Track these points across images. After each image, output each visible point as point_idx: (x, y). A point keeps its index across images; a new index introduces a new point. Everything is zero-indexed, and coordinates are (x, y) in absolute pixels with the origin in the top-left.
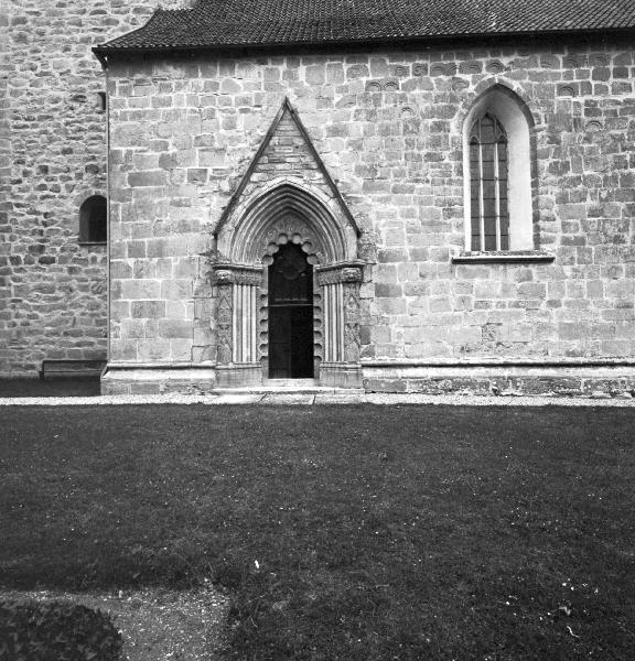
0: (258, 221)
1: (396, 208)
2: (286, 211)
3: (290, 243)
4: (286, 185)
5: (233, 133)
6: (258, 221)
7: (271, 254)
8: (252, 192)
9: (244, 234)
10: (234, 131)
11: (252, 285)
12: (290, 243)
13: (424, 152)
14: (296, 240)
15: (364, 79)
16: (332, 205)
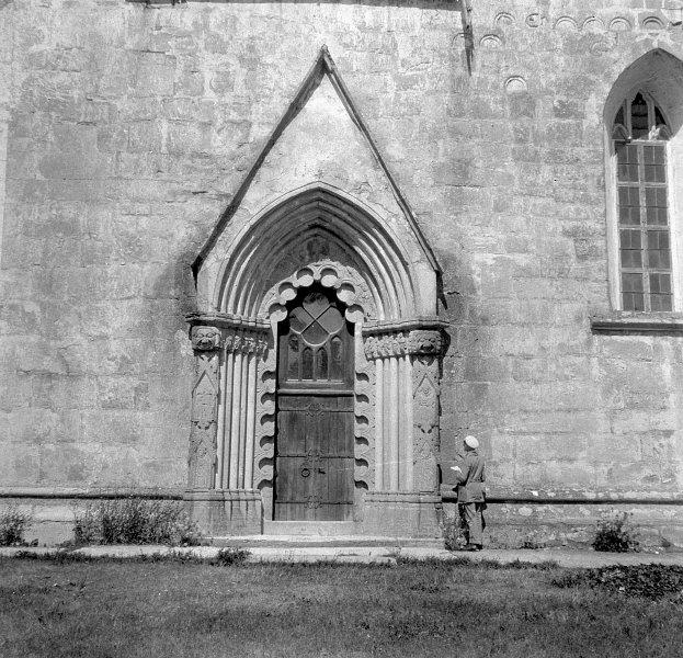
2: (316, 231)
3: (317, 284)
5: (228, 98)
7: (283, 302)
8: (257, 203)
13: (544, 151)
14: (328, 281)
16: (396, 225)
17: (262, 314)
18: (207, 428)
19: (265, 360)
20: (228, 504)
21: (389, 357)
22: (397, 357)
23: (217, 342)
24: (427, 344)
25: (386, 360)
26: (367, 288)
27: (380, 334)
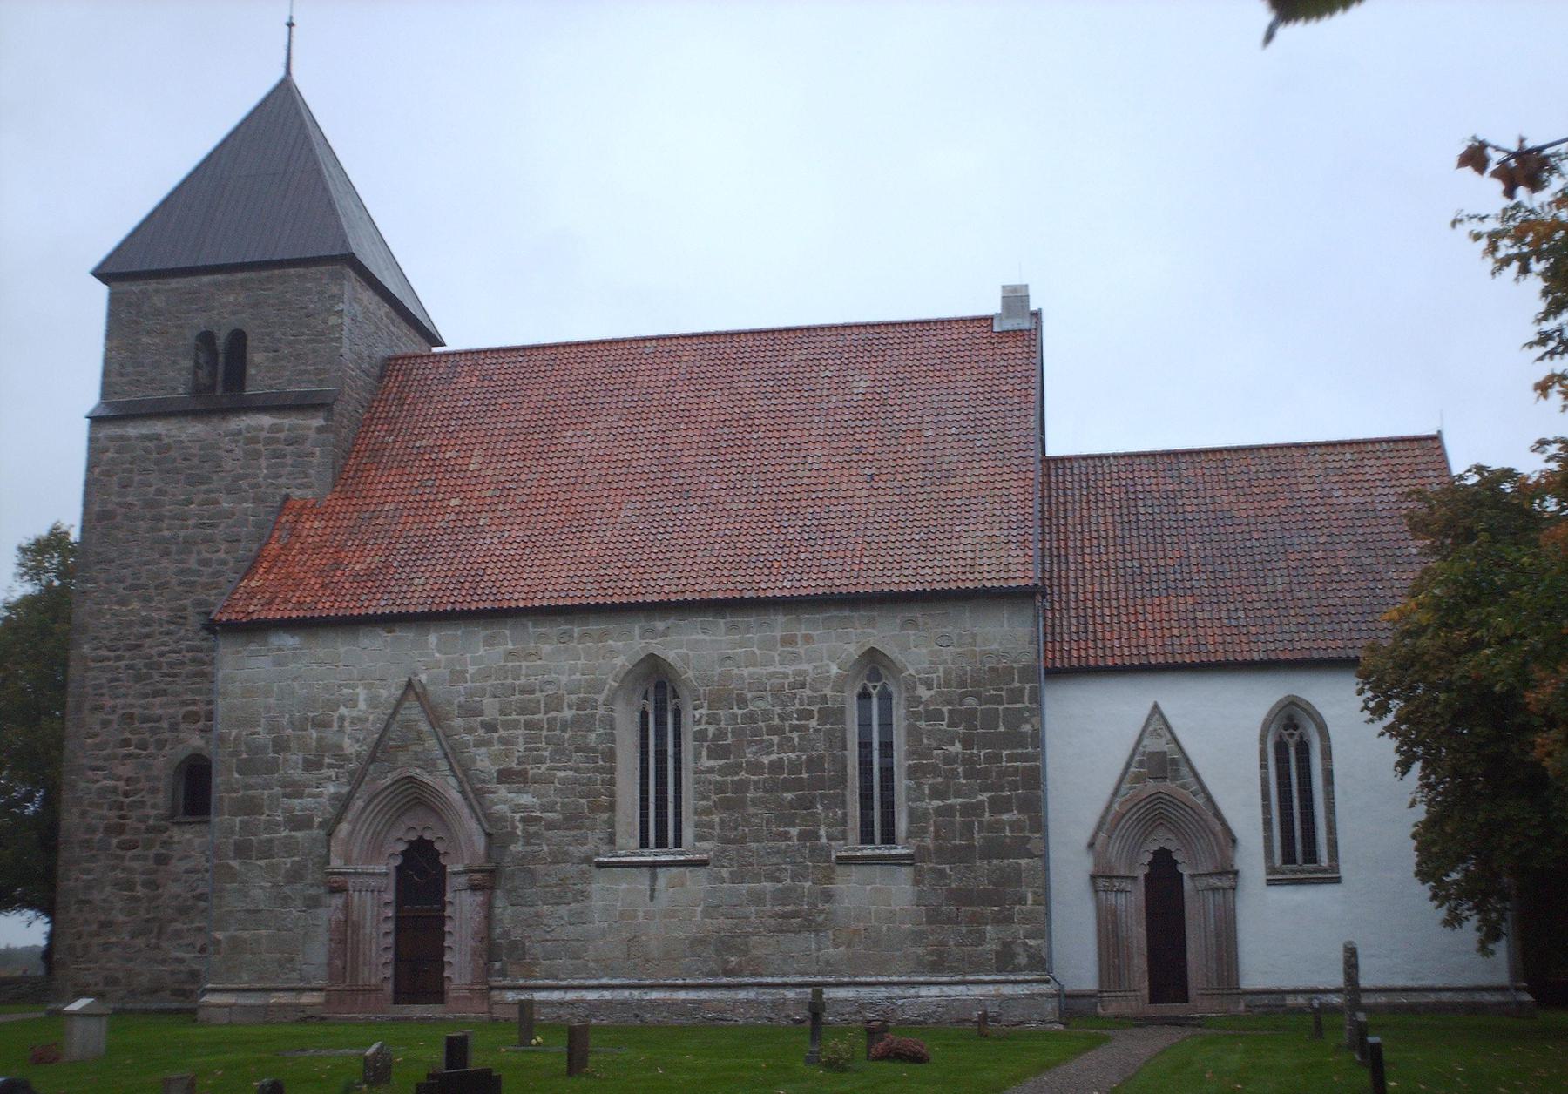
0: (380, 816)
1: (535, 800)
3: (421, 838)
4: (411, 777)
6: (380, 816)
9: (362, 832)
11: (372, 891)
12: (421, 838)
14: (428, 836)
15: (500, 649)
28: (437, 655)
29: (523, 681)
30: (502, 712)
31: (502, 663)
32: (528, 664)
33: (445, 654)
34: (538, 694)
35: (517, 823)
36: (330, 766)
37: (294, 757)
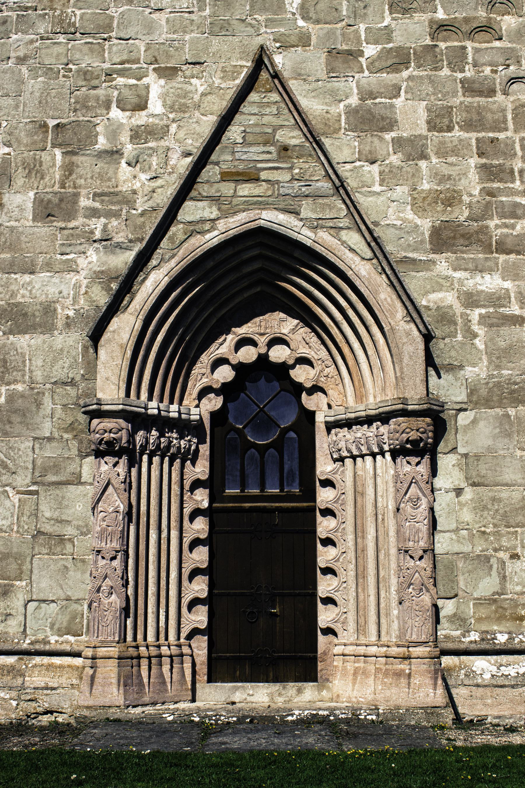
1: (508, 284)
10: (144, 113)
17: (189, 400)
18: (113, 558)
19: (193, 464)
20: (144, 663)
21: (362, 456)
22: (374, 455)
23: (124, 440)
24: (414, 435)
25: (359, 460)
26: (330, 362)
27: (349, 424)
28: (301, 23)
29: (469, 73)
30: (432, 126)
31: (428, 41)
32: (477, 45)
33: (318, 22)
34: (500, 97)
35: (475, 328)
36: (94, 213)
37: (18, 199)
